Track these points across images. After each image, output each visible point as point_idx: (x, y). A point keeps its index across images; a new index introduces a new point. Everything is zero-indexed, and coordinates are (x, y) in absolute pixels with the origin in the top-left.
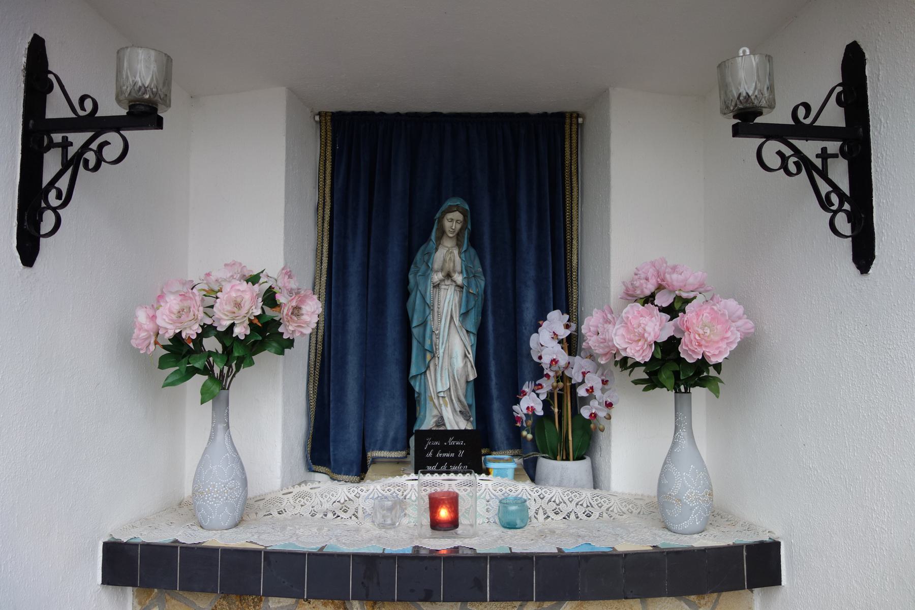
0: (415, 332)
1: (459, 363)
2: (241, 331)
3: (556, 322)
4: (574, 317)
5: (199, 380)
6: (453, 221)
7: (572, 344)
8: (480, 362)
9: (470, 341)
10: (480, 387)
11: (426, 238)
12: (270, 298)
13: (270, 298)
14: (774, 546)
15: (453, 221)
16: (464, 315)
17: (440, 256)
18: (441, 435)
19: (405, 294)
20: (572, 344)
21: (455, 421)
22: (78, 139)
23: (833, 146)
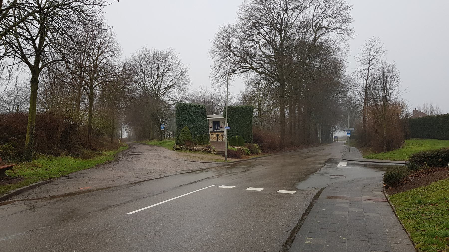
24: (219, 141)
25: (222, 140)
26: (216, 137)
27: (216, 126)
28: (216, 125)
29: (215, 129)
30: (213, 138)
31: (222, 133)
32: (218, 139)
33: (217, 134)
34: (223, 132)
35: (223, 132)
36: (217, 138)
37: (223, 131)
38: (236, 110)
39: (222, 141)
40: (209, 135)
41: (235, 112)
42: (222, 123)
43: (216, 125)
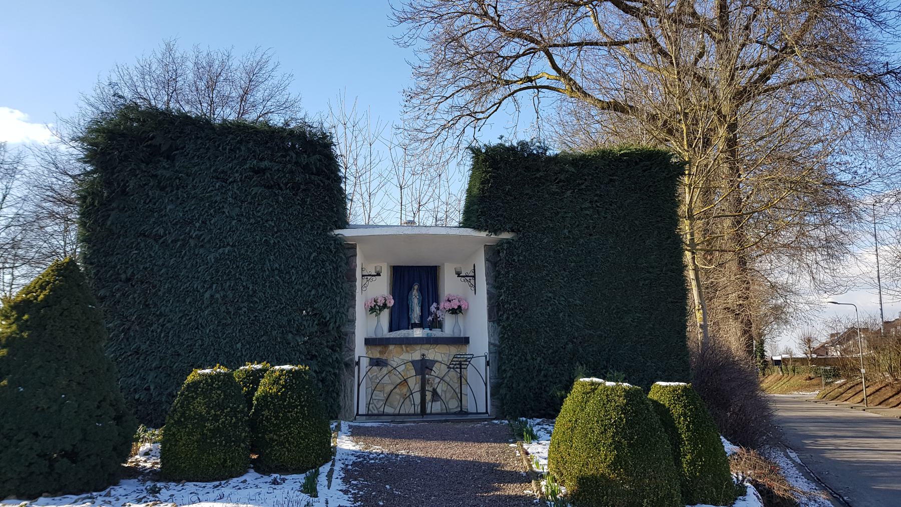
0: (410, 306)
1: (418, 312)
2: (381, 305)
3: (435, 305)
4: (438, 304)
5: (375, 313)
6: (416, 287)
7: (438, 309)
8: (422, 311)
9: (420, 308)
10: (422, 317)
11: (411, 290)
12: (386, 300)
13: (386, 300)
14: (469, 338)
15: (416, 287)
16: (419, 303)
17: (414, 293)
18: (415, 323)
19: (408, 300)
20: (438, 309)
21: (417, 322)
22: (369, 277)
23: (471, 278)
24: (436, 407)
25: (453, 405)
26: (414, 383)
27: (416, 301)
28: (415, 293)
29: (409, 319)
30: (388, 389)
31: (453, 350)
32: (429, 396)
33: (417, 356)
34: (466, 341)
35: (466, 341)
36: (417, 388)
37: (462, 336)
38: (562, 177)
39: (462, 412)
40: (351, 365)
41: (554, 188)
42: (459, 274)
43: (410, 289)
